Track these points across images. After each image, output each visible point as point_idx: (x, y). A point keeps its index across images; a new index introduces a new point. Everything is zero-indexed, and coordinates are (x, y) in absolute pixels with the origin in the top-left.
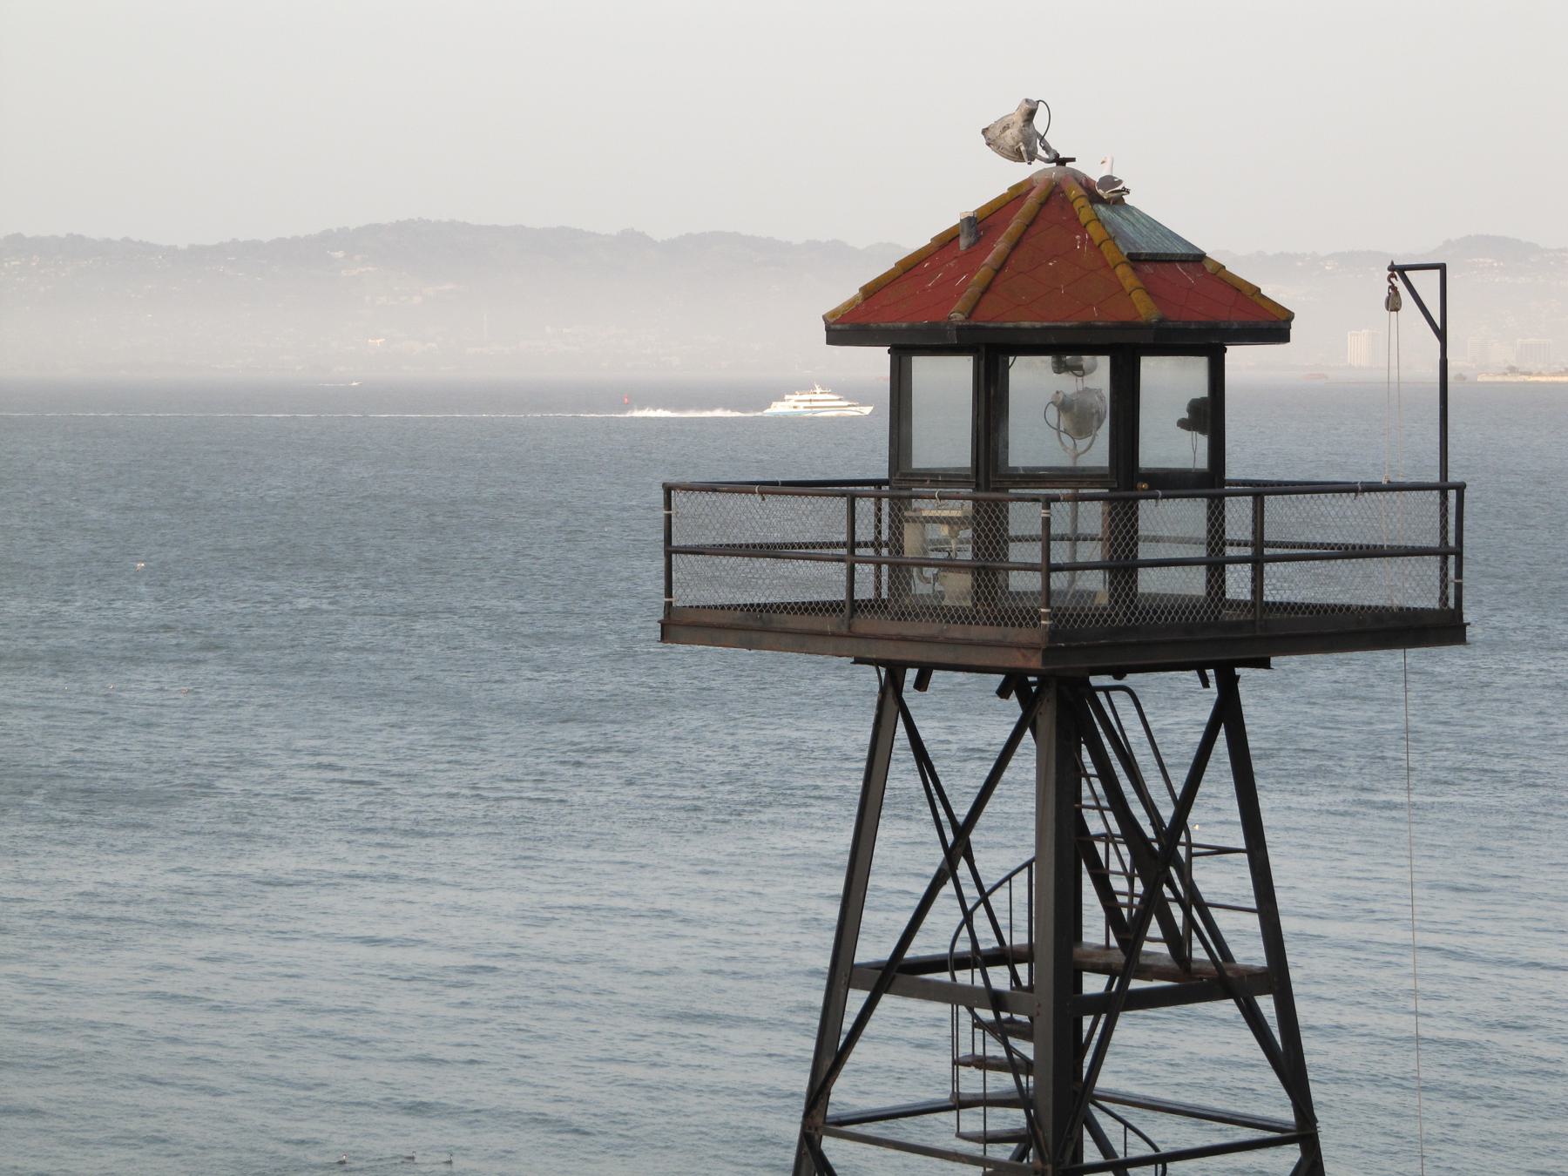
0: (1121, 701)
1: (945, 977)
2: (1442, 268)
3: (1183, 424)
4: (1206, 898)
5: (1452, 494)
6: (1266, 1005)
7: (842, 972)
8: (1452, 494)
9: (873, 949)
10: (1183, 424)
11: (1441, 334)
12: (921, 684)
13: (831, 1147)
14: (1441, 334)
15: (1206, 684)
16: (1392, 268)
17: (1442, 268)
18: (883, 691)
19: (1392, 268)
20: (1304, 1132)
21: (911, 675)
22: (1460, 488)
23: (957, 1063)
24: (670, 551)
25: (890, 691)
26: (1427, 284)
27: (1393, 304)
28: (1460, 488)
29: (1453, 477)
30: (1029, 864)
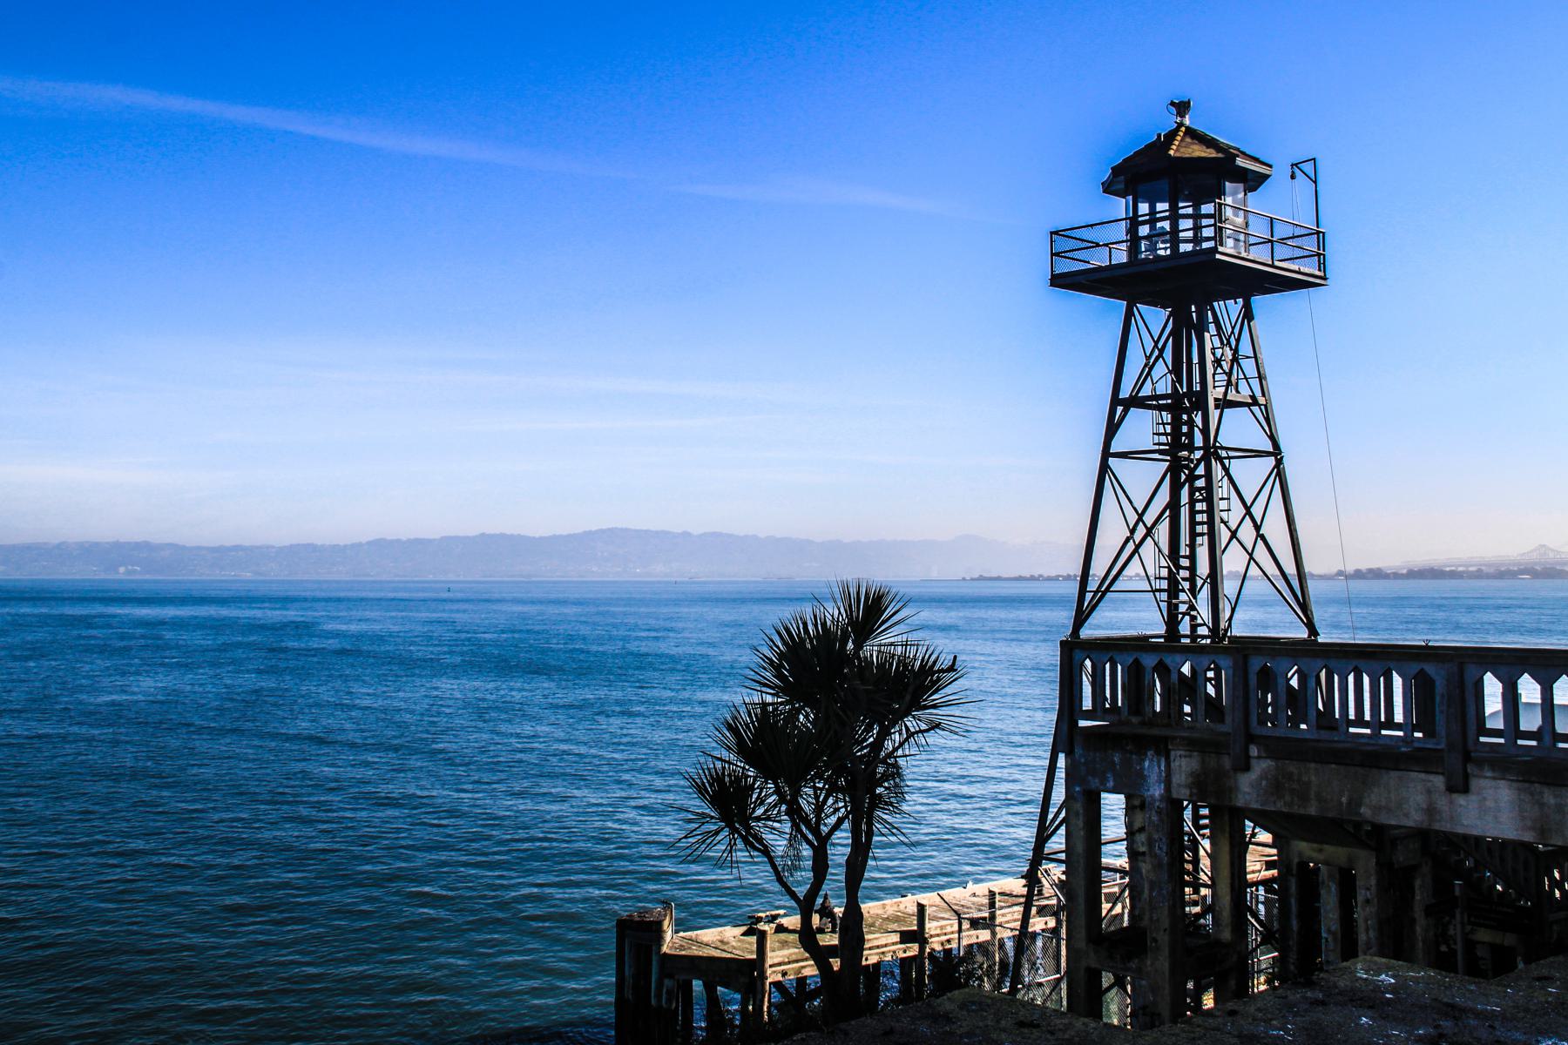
2: (1314, 159)
5: (1321, 235)
7: (1115, 401)
8: (1321, 235)
9: (1125, 393)
11: (1315, 182)
13: (1111, 461)
14: (1315, 182)
15: (1236, 303)
16: (1292, 165)
20: (1276, 452)
23: (1154, 434)
24: (1052, 254)
26: (1308, 168)
27: (1293, 177)
28: (1323, 233)
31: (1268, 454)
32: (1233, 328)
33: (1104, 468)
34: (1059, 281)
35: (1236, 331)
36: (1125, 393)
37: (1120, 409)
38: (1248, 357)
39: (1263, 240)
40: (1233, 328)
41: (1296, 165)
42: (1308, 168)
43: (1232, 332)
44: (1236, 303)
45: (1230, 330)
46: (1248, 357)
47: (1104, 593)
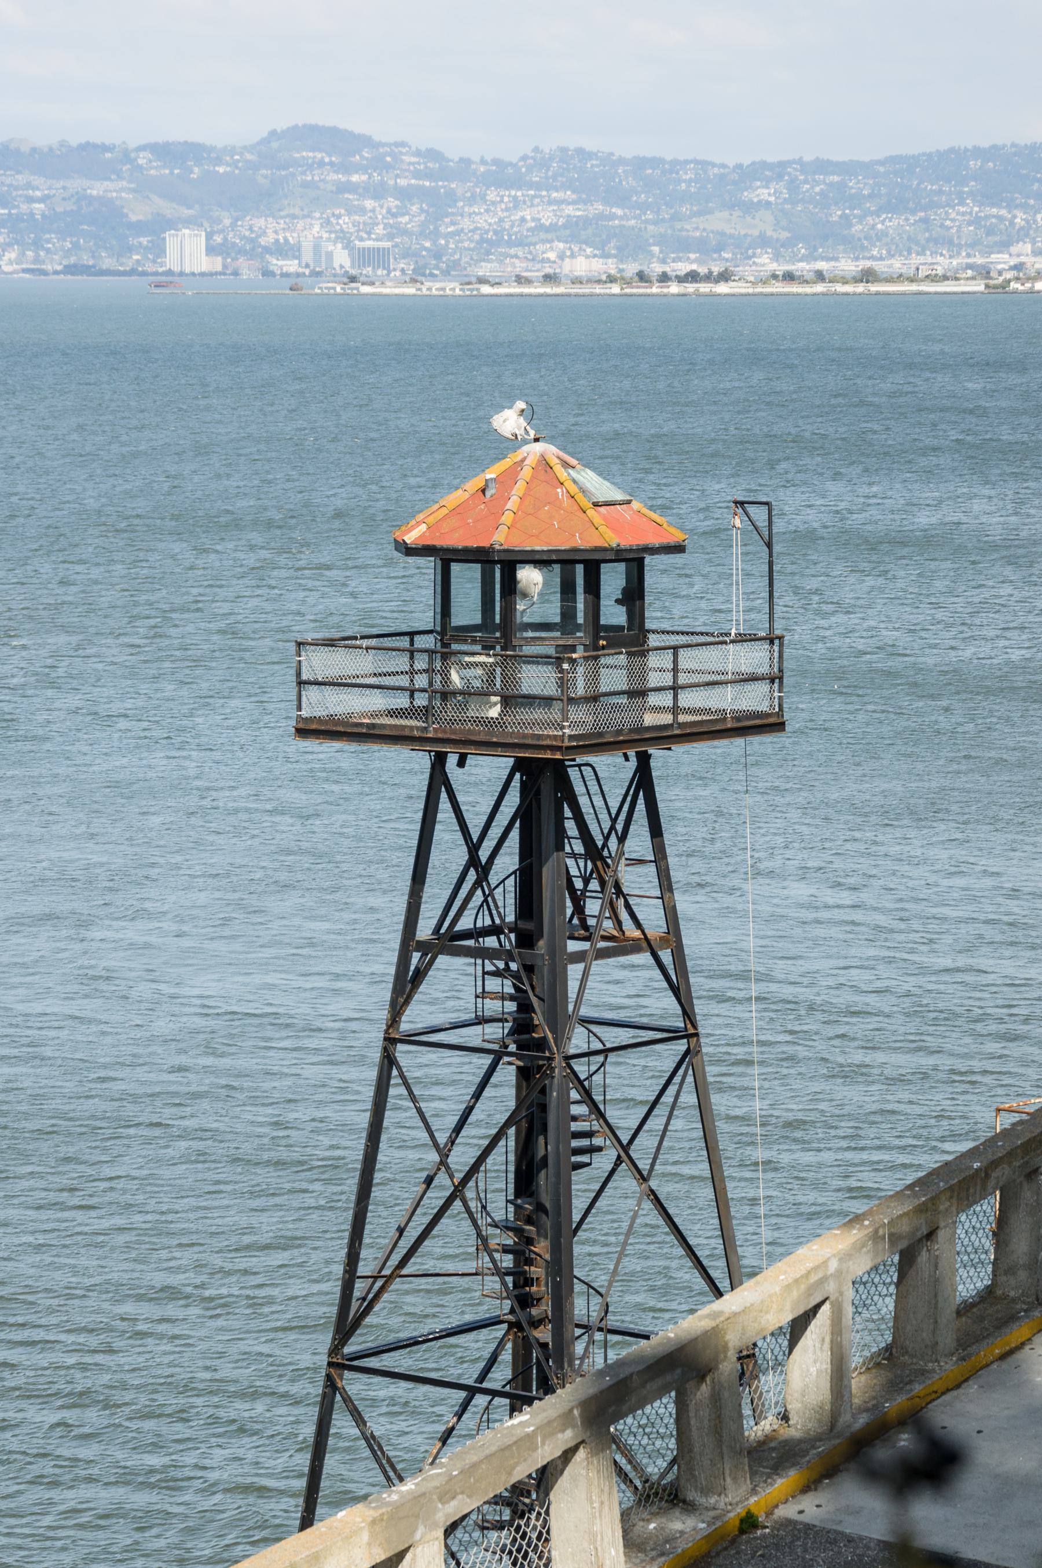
0: (587, 771)
1: (470, 943)
3: (617, 601)
4: (625, 891)
6: (666, 956)
9: (424, 931)
10: (617, 601)
11: (769, 545)
12: (461, 763)
14: (769, 545)
15: (627, 759)
17: (766, 503)
18: (433, 767)
19: (736, 502)
21: (452, 760)
22: (781, 638)
24: (301, 683)
25: (438, 767)
28: (781, 638)
29: (777, 632)
30: (514, 872)
31: (673, 1035)
32: (614, 820)
33: (389, 1061)
34: (306, 730)
35: (619, 827)
36: (424, 931)
37: (416, 956)
38: (641, 862)
39: (373, 1363)
40: (614, 820)
41: (741, 504)
42: (759, 514)
43: (612, 828)
44: (627, 759)
45: (606, 825)
46: (641, 862)
47: (389, 1279)
